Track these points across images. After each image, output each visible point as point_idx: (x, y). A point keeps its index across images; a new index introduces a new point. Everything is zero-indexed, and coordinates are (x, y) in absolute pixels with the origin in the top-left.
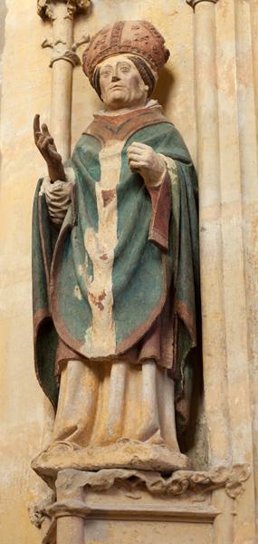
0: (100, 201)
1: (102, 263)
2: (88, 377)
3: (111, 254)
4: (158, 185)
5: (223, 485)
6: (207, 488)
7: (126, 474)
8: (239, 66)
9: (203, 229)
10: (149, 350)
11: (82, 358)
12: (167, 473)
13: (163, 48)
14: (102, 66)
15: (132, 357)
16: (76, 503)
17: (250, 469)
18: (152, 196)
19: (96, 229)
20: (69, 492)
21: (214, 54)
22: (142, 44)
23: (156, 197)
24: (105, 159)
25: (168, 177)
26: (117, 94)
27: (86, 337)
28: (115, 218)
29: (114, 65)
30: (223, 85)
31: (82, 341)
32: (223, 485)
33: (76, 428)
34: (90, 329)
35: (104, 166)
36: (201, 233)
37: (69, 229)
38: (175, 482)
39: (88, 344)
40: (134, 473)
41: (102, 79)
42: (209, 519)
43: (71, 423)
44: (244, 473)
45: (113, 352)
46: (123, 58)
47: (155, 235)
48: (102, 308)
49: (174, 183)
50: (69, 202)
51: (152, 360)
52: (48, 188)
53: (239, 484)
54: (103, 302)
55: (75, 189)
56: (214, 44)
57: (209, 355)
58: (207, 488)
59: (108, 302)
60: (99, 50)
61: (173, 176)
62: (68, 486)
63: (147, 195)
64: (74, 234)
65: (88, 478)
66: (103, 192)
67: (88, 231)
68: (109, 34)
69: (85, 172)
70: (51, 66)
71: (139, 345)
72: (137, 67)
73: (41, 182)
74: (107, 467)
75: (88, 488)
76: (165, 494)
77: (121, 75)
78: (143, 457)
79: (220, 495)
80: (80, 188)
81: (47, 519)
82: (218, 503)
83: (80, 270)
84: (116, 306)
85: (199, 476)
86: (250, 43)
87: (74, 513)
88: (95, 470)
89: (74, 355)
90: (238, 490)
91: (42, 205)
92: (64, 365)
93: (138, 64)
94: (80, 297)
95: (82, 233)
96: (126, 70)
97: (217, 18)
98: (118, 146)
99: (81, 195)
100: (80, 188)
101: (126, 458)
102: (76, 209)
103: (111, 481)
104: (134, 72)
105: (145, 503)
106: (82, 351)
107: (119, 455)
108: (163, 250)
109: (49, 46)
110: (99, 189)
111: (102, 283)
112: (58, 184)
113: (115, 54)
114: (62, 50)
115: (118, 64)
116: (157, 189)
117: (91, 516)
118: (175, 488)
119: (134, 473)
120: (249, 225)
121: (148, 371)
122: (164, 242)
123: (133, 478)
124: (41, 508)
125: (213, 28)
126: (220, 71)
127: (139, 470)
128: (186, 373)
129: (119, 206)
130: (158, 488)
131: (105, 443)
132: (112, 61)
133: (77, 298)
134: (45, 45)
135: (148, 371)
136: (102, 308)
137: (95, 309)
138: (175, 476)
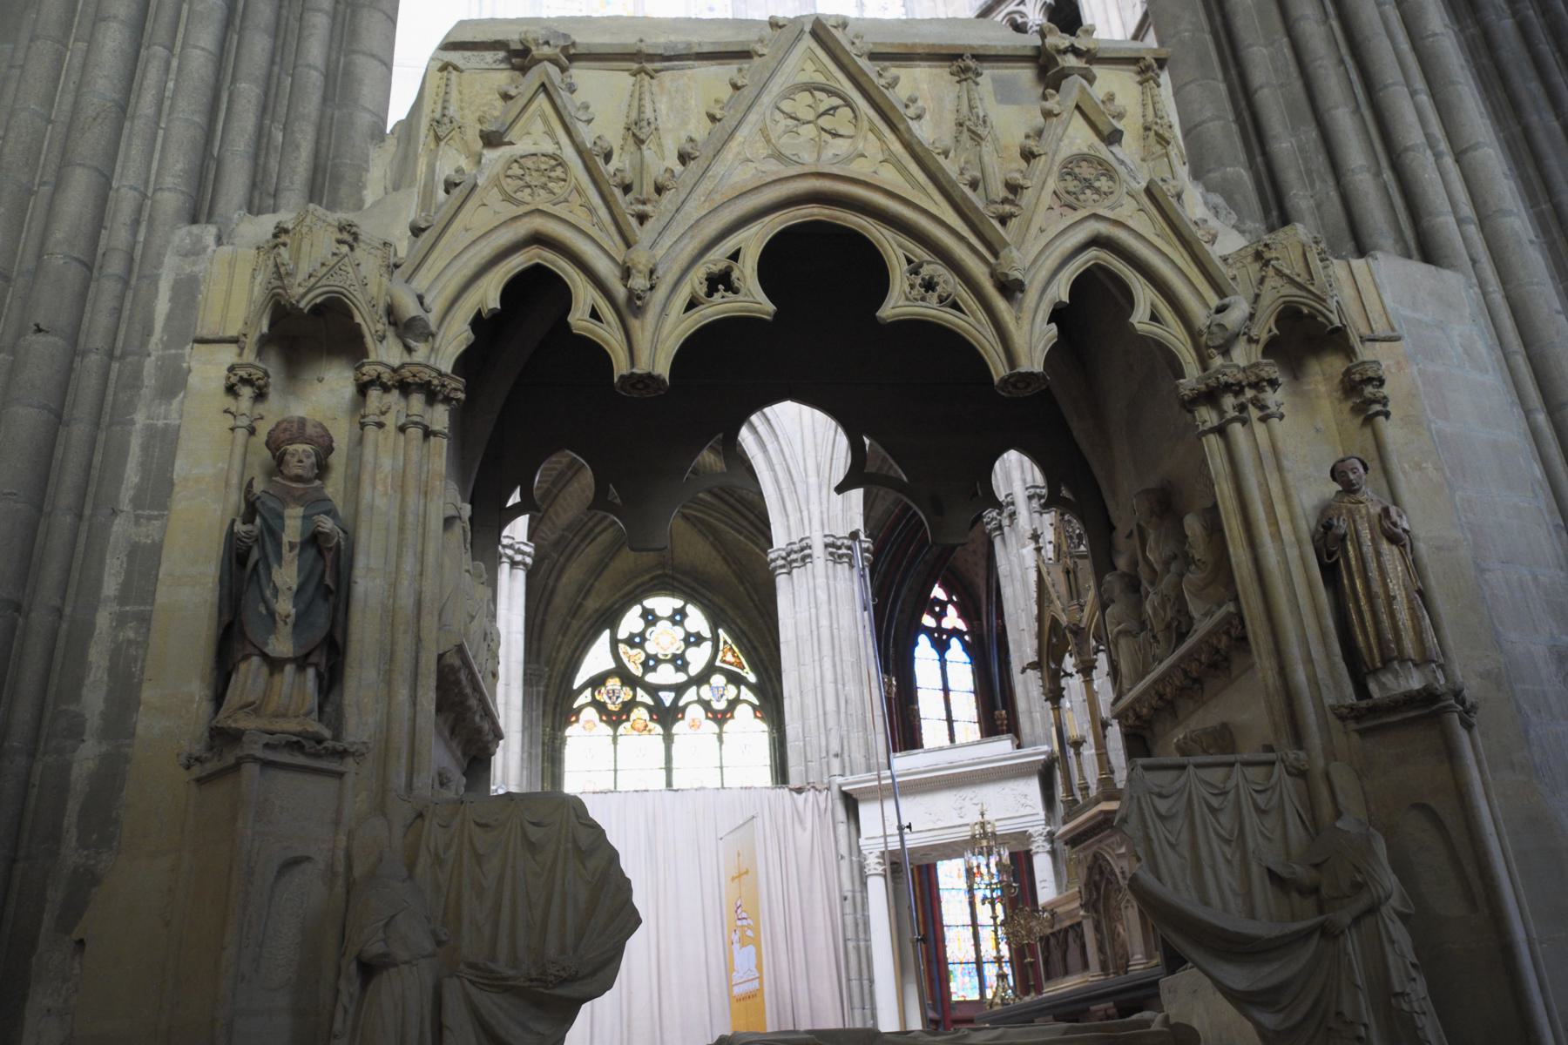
0: (285, 548)
1: (289, 593)
2: (265, 670)
3: (295, 587)
4: (330, 546)
5: (353, 754)
6: (342, 754)
7: (295, 739)
8: (392, 478)
9: (356, 583)
10: (314, 659)
11: (265, 657)
12: (320, 740)
13: (331, 446)
14: (291, 448)
15: (301, 663)
16: (259, 753)
17: (370, 745)
18: (326, 553)
19: (280, 567)
20: (255, 746)
21: (375, 464)
22: (321, 440)
23: (329, 556)
24: (290, 517)
25: (339, 543)
26: (300, 472)
27: (269, 641)
28: (296, 562)
29: (300, 450)
30: (380, 488)
31: (267, 644)
32: (353, 754)
33: (254, 703)
34: (272, 637)
35: (288, 522)
36: (352, 585)
37: (256, 564)
38: (325, 748)
39: (271, 647)
40: (299, 739)
41: (288, 457)
42: (340, 775)
43: (251, 699)
44: (367, 748)
45: (291, 655)
46: (307, 447)
47: (328, 581)
48: (286, 623)
49: (343, 548)
50: (257, 540)
51: (316, 665)
52: (239, 527)
53: (363, 754)
54: (288, 620)
55: (262, 532)
56: (376, 457)
57: (352, 668)
58: (342, 754)
59: (290, 621)
60: (287, 435)
61: (342, 543)
62: (256, 743)
63: (320, 553)
64: (261, 567)
65: (267, 738)
66: (290, 542)
67: (275, 568)
68: (295, 425)
69: (271, 522)
70: (232, 429)
71: (307, 655)
72: (316, 456)
73: (233, 522)
74: (282, 733)
75: (267, 746)
76: (317, 756)
77: (305, 460)
78: (310, 729)
79: (350, 761)
80: (265, 534)
81: (198, 764)
82: (350, 765)
83: (268, 593)
84: (295, 626)
85: (339, 746)
86: (401, 464)
87: (256, 759)
88: (272, 733)
89: (257, 652)
90: (361, 758)
91: (231, 533)
92: (247, 657)
93: (317, 455)
94: (264, 612)
95: (269, 568)
96: (308, 457)
97: (380, 439)
98: (299, 511)
99: (267, 539)
100: (265, 534)
101: (299, 729)
102: (263, 549)
103: (283, 743)
104: (313, 459)
105: (300, 760)
106: (266, 650)
107: (292, 726)
108: (328, 591)
109: (230, 413)
110: (285, 539)
111: (285, 606)
112: (248, 527)
113: (302, 443)
114: (244, 421)
115: (304, 451)
116: (330, 549)
117: (267, 764)
118: (323, 752)
119: (299, 739)
120: (386, 586)
121: (311, 672)
122: (332, 587)
123: (298, 742)
124: (198, 754)
125: (377, 446)
126: (378, 477)
127: (305, 738)
128: (326, 676)
129: (300, 555)
130: (313, 750)
131: (276, 715)
132: (300, 447)
133: (261, 613)
134: (226, 411)
135: (311, 672)
136: (286, 623)
137: (280, 624)
138: (326, 744)
